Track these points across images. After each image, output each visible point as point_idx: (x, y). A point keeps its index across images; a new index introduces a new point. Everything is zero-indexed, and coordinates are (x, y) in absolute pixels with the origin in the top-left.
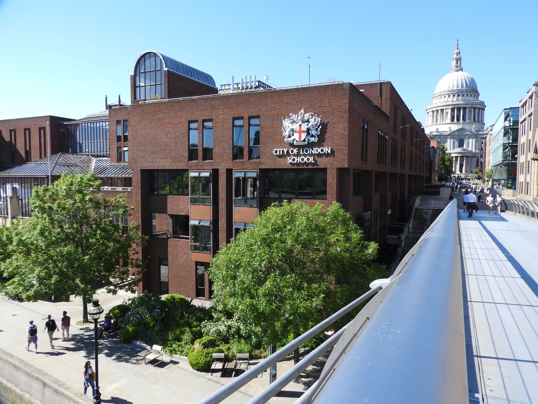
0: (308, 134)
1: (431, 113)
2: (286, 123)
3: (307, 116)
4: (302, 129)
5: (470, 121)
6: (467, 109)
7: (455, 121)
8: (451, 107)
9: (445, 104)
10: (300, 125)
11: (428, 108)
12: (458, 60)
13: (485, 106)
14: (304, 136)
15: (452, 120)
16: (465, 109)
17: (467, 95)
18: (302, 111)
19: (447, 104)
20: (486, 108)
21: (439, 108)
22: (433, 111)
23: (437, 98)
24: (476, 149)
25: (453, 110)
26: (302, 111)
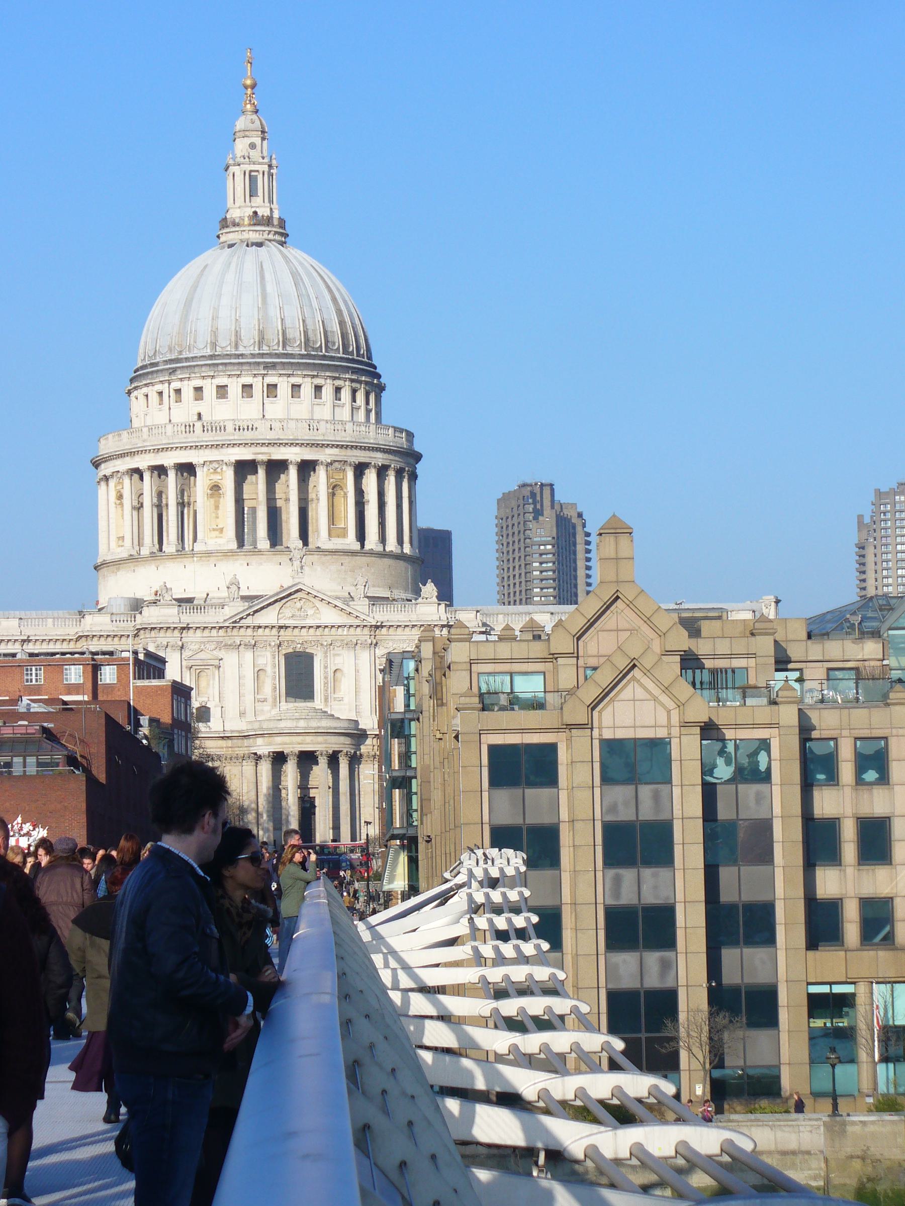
3: (27, 827)
5: (337, 543)
7: (263, 543)
8: (233, 459)
9: (198, 435)
13: (418, 457)
16: (306, 468)
17: (318, 388)
18: (19, 820)
19: (209, 438)
21: (169, 460)
23: (152, 391)
26: (19, 820)
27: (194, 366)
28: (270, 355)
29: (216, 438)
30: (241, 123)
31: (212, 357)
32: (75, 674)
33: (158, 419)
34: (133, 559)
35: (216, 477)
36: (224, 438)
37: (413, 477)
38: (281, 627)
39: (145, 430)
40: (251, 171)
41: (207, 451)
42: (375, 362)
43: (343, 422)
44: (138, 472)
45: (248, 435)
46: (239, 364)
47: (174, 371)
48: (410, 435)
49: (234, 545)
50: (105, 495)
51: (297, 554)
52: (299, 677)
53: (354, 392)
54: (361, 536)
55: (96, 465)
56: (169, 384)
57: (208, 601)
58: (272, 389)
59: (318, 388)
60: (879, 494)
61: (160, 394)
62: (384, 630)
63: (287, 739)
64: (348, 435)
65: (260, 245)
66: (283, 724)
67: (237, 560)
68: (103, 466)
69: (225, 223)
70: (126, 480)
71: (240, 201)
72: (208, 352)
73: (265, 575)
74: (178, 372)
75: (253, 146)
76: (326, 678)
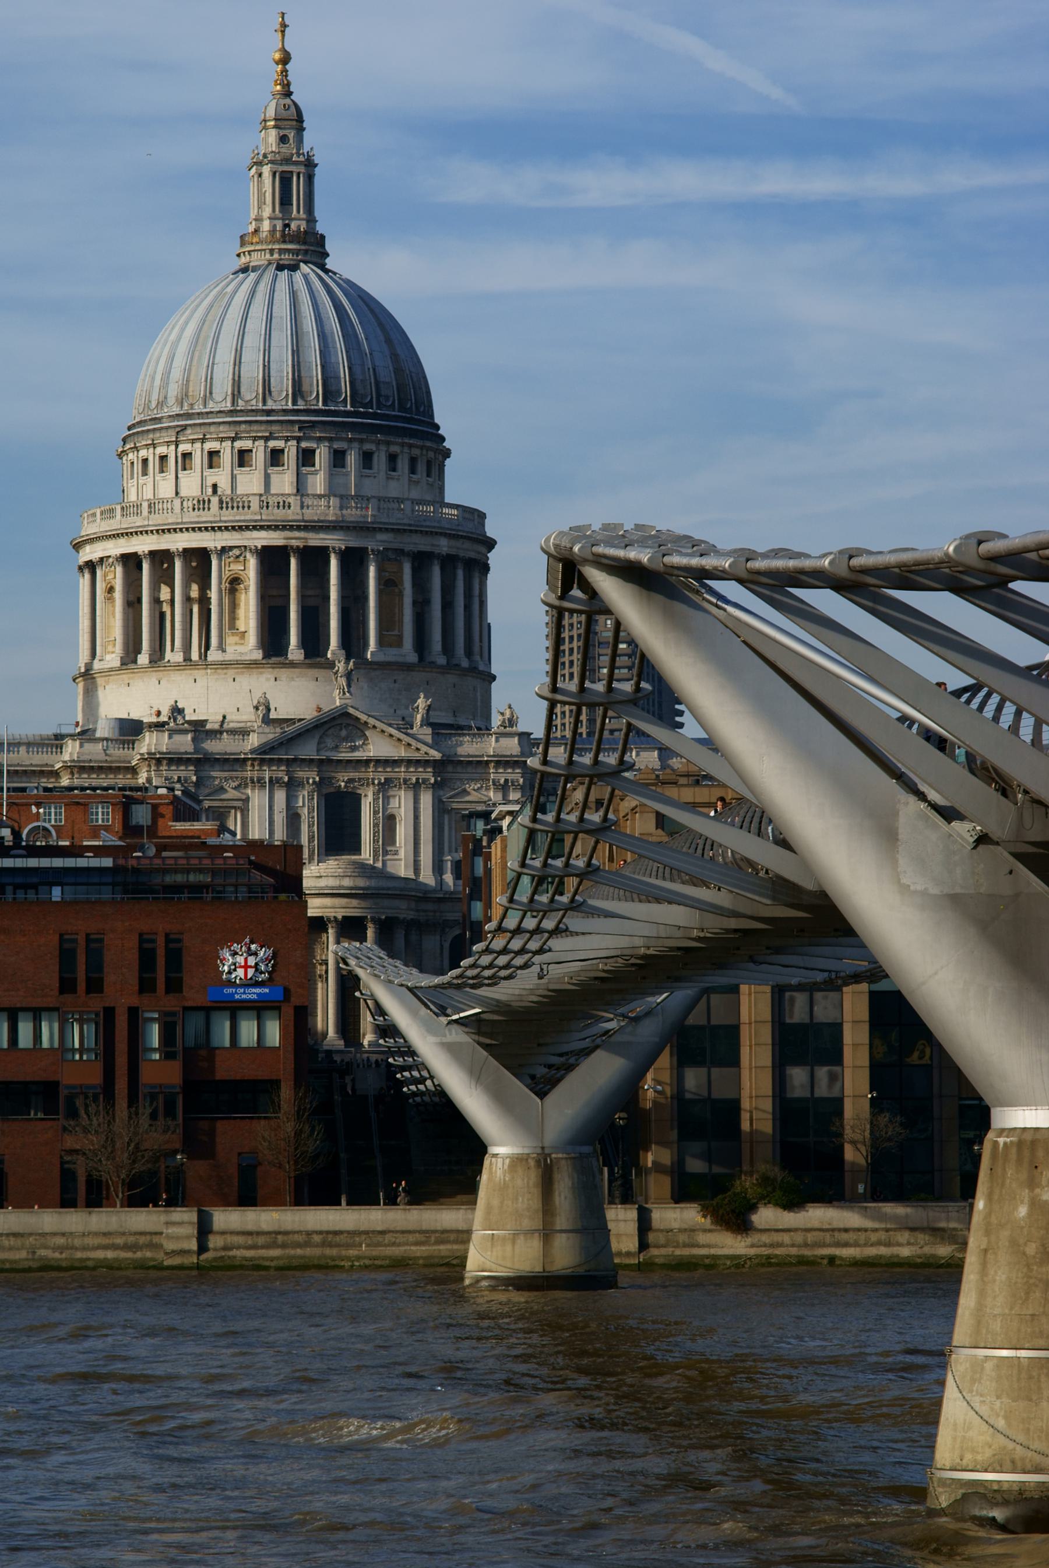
0: (257, 970)
1: (117, 576)
2: (226, 954)
3: (253, 947)
4: (249, 964)
5: (391, 655)
10: (246, 960)
11: (90, 529)
12: (294, 178)
13: (491, 544)
14: (251, 972)
15: (273, 642)
19: (229, 516)
20: (494, 558)
22: (131, 562)
24: (438, 868)
25: (272, 561)
26: (247, 940)
27: (210, 424)
28: (307, 412)
29: (237, 518)
31: (232, 413)
32: (102, 815)
35: (237, 567)
36: (248, 517)
37: (486, 568)
38: (321, 761)
39: (145, 505)
40: (283, 172)
41: (226, 535)
42: (436, 421)
43: (399, 500)
45: (279, 514)
46: (268, 422)
47: (185, 428)
48: (482, 516)
49: (258, 655)
51: (341, 666)
53: (413, 461)
55: (77, 546)
56: (177, 446)
57: (225, 726)
59: (367, 459)
61: (163, 458)
62: (450, 768)
63: (328, 901)
65: (294, 268)
66: (322, 883)
67: (261, 673)
68: (88, 548)
70: (119, 570)
71: (267, 211)
72: (228, 406)
74: (189, 431)
75: (283, 139)
76: (376, 825)
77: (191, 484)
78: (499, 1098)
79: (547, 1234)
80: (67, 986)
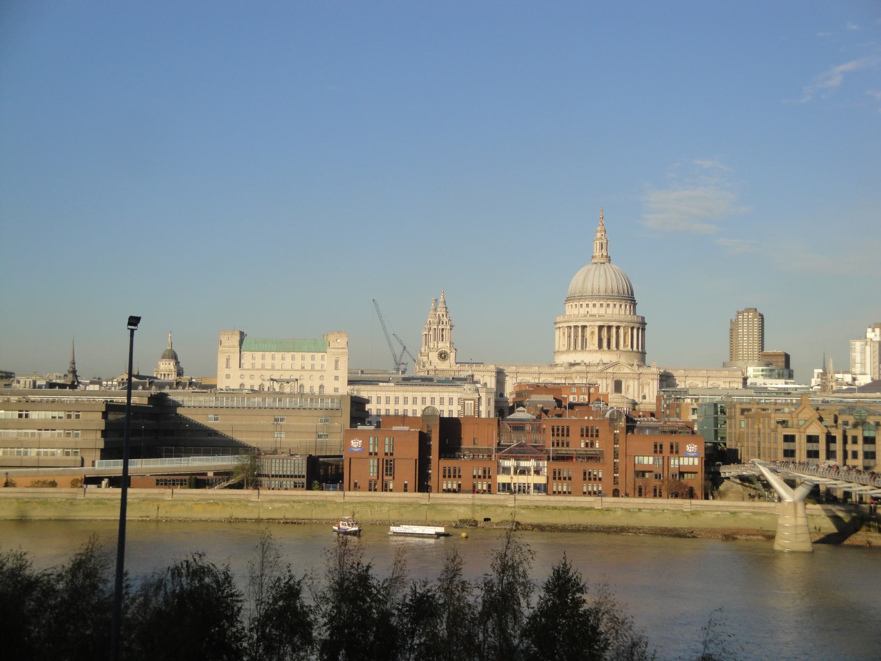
5: (626, 349)
6: (621, 331)
15: (600, 346)
16: (618, 328)
20: (646, 327)
21: (580, 324)
23: (574, 305)
25: (601, 328)
30: (599, 229)
32: (584, 390)
33: (574, 312)
34: (568, 350)
37: (643, 329)
44: (570, 327)
50: (557, 332)
52: (618, 387)
54: (632, 347)
55: (556, 323)
58: (608, 305)
60: (738, 313)
64: (629, 318)
69: (593, 257)
73: (607, 357)
77: (583, 311)
78: (785, 490)
79: (796, 516)
80: (655, 452)
